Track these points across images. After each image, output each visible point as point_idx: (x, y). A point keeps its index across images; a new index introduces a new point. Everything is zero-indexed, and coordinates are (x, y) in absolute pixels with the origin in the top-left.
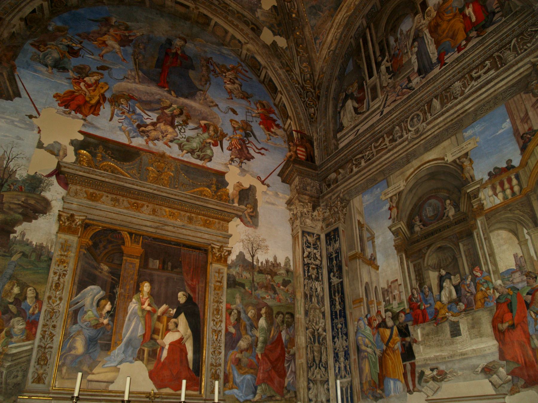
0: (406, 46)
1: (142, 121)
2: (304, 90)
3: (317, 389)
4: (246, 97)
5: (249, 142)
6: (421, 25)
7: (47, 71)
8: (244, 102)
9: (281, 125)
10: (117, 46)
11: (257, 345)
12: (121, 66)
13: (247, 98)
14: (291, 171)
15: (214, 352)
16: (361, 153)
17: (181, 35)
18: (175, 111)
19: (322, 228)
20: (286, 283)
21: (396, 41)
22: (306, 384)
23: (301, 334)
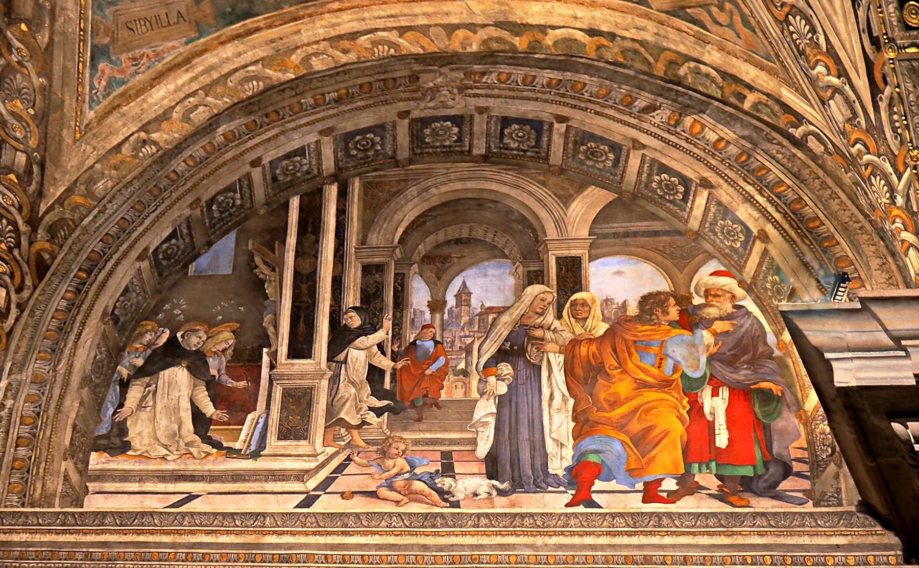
0: (468, 350)
6: (541, 327)
21: (436, 306)
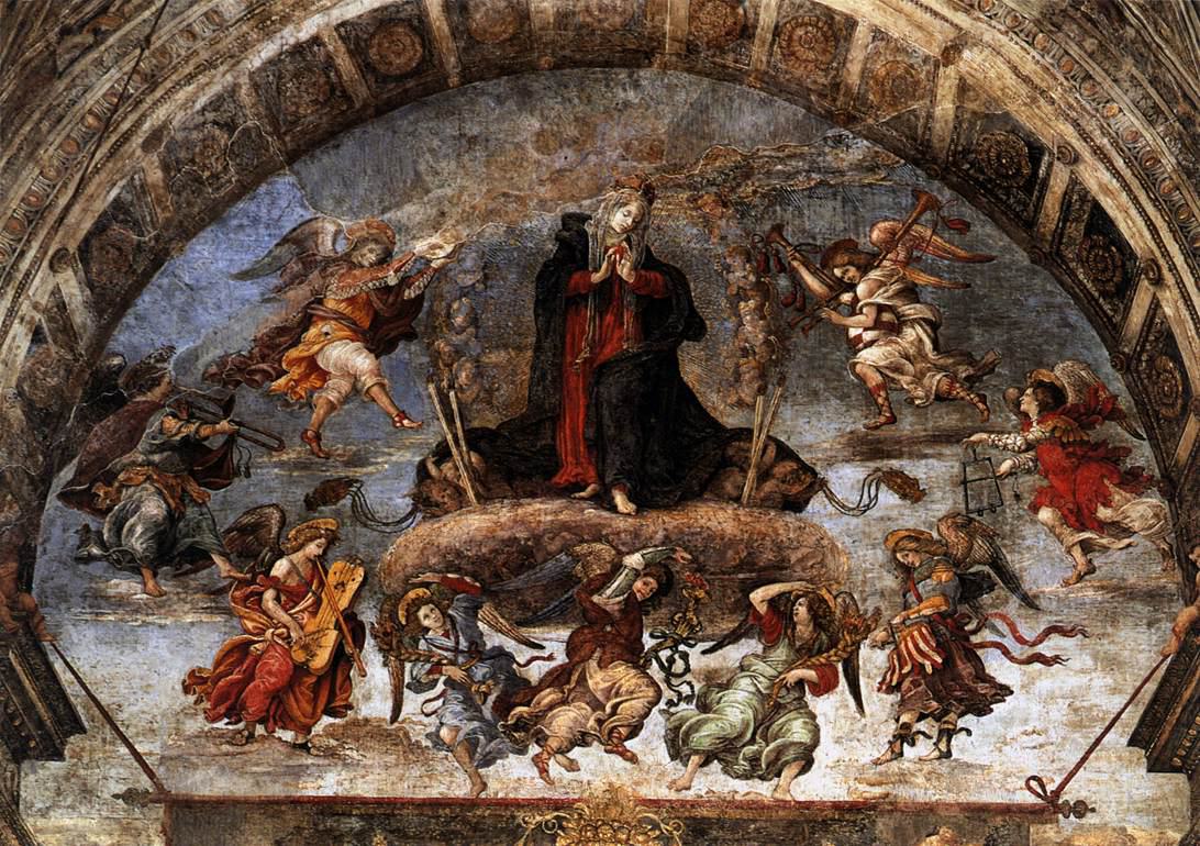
10: (362, 362)
18: (638, 584)
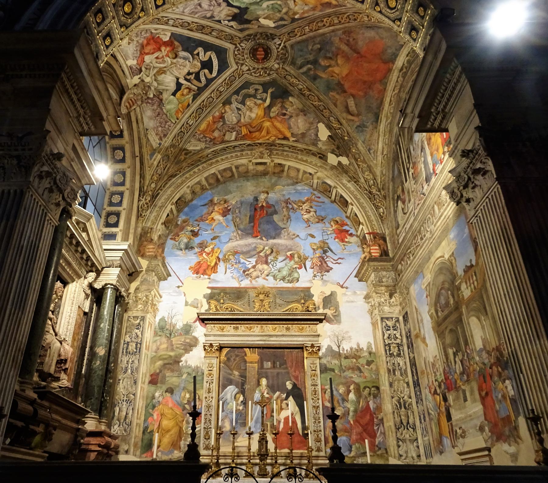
1: (246, 267)
2: (371, 195)
3: (407, 446)
4: (321, 220)
5: (327, 257)
7: (182, 253)
8: (320, 225)
9: (354, 233)
10: (221, 218)
11: (349, 414)
12: (226, 232)
13: (322, 220)
14: (367, 269)
15: (315, 422)
16: (409, 248)
17: (264, 190)
19: (400, 310)
20: (369, 363)
22: (395, 442)
23: (387, 402)
